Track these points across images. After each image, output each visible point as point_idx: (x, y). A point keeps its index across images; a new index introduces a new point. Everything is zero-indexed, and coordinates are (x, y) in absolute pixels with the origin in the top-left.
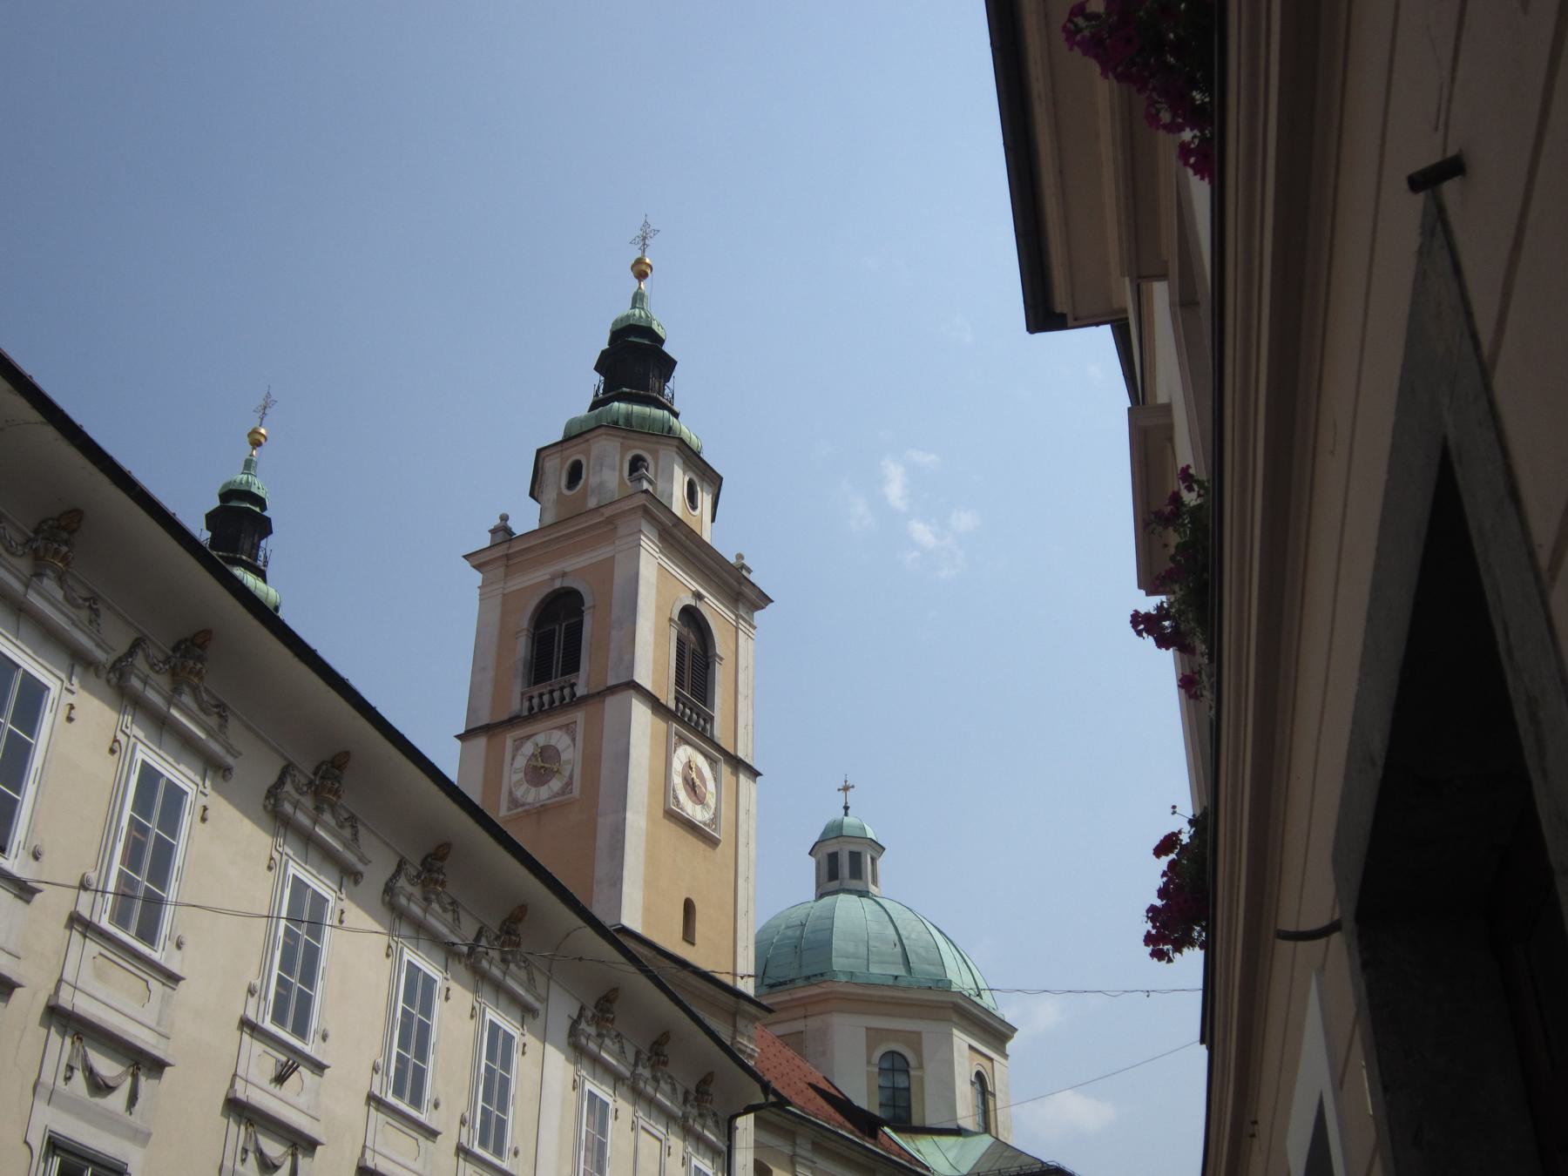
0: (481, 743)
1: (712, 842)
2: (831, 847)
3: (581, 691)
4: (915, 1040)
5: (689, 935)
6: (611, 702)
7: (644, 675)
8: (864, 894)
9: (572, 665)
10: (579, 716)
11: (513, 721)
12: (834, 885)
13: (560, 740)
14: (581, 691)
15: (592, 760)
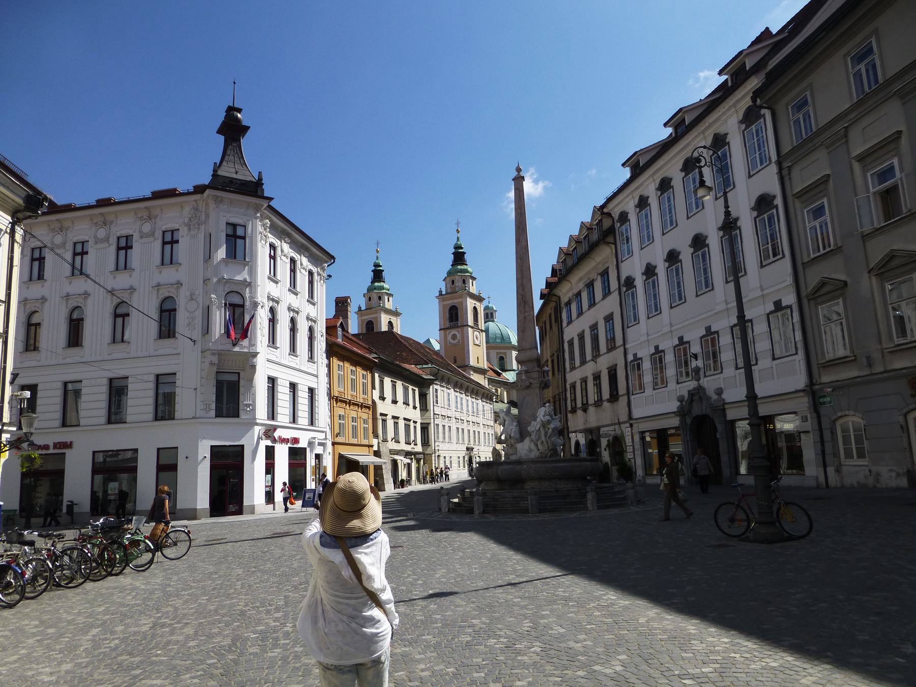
0: (442, 331)
1: (480, 346)
2: (487, 311)
3: (459, 325)
4: (505, 354)
5: (478, 363)
6: (465, 328)
7: (469, 324)
8: (493, 321)
9: (457, 320)
10: (459, 330)
11: (448, 328)
12: (488, 320)
13: (457, 333)
14: (459, 325)
15: (463, 337)
